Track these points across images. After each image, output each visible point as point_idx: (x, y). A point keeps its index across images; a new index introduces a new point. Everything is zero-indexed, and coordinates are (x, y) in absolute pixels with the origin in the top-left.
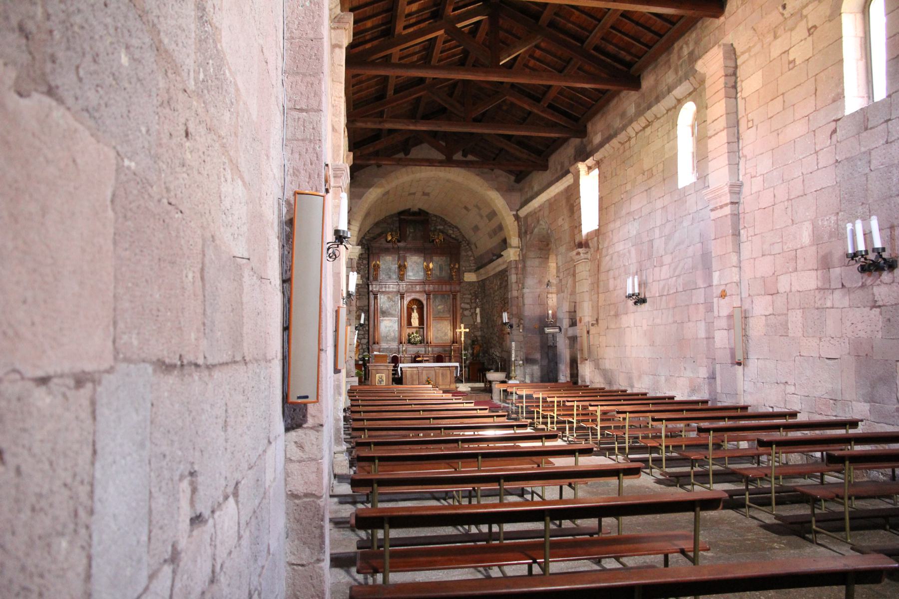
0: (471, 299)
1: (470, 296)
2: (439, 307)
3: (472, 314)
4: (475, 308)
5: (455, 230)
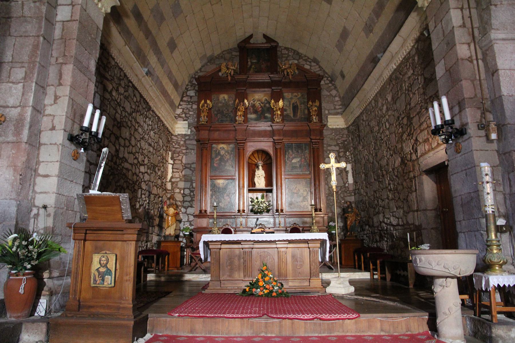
1: (337, 148)
2: (294, 161)
5: (313, 64)
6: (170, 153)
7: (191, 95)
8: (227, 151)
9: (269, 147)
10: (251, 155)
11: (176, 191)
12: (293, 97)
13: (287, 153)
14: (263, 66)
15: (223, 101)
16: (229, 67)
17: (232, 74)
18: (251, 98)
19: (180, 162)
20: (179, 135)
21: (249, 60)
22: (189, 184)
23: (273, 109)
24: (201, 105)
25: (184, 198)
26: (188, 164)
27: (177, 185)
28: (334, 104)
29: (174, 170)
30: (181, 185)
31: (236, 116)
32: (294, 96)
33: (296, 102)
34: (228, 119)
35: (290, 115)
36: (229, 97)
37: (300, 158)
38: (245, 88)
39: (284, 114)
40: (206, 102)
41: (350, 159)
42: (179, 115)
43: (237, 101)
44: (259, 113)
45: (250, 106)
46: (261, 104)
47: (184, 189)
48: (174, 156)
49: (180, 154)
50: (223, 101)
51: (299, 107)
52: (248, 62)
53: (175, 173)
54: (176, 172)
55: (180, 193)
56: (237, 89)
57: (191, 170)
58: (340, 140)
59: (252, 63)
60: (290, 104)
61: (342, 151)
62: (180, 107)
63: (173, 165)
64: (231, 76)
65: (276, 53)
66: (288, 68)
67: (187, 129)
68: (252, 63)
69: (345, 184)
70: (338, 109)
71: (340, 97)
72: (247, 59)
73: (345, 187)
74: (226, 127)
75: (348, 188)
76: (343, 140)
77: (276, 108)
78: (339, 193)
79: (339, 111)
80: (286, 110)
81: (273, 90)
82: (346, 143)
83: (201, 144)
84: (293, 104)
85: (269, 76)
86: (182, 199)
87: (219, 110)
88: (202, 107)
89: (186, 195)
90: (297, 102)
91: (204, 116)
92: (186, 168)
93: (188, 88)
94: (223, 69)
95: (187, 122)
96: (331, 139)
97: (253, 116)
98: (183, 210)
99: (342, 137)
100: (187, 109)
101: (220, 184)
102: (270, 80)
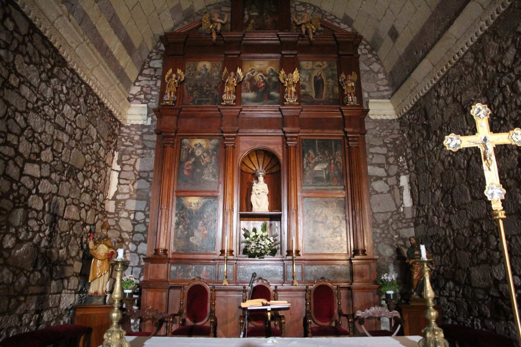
0: (387, 157)
1: (384, 150)
2: (317, 168)
3: (392, 188)
4: (398, 175)
6: (116, 154)
7: (156, 66)
8: (207, 151)
9: (277, 144)
10: (245, 158)
11: (122, 216)
12: (315, 67)
13: (306, 155)
14: (269, 21)
15: (204, 72)
16: (213, 19)
17: (219, 28)
18: (247, 67)
19: (132, 168)
20: (132, 125)
21: (246, 12)
22: (144, 203)
23: (283, 84)
24: (167, 76)
25: (134, 228)
26: (145, 172)
27: (124, 205)
28: (378, 84)
29: (122, 181)
30: (132, 205)
31: (222, 93)
32: (317, 66)
33: (320, 76)
34: (210, 99)
35: (310, 94)
36: (213, 66)
37: (327, 164)
38: (238, 52)
39: (301, 93)
40: (175, 72)
41: (406, 167)
42: (135, 96)
43: (226, 70)
44: (260, 90)
45: (246, 79)
46: (264, 78)
47: (135, 212)
48: (123, 159)
49: (133, 156)
50: (204, 72)
51: (325, 83)
52: (244, 15)
53: (122, 186)
54: (125, 184)
55: (128, 218)
56: (226, 53)
57: (148, 181)
58: (389, 139)
59: (251, 17)
60: (310, 78)
61: (392, 156)
62: (137, 84)
63: (120, 172)
64: (217, 33)
65: (290, 10)
66: (307, 22)
67: (146, 116)
68: (251, 17)
69: (398, 208)
70: (383, 91)
71: (385, 73)
72: (244, 10)
73: (398, 212)
74: (207, 111)
75: (404, 215)
76: (393, 139)
77: (288, 82)
78: (390, 223)
79: (386, 93)
80: (304, 87)
81: (282, 55)
82: (398, 142)
83: (164, 137)
84: (315, 77)
85: (278, 35)
86: (132, 229)
87: (196, 86)
88: (168, 79)
89: (138, 223)
90: (322, 75)
91: (170, 93)
92: (141, 178)
93: (152, 57)
94: (204, 23)
95: (145, 105)
96: (375, 136)
97: (251, 95)
98: (132, 247)
99: (391, 134)
100: (149, 86)
101: (193, 204)
102: (279, 42)
